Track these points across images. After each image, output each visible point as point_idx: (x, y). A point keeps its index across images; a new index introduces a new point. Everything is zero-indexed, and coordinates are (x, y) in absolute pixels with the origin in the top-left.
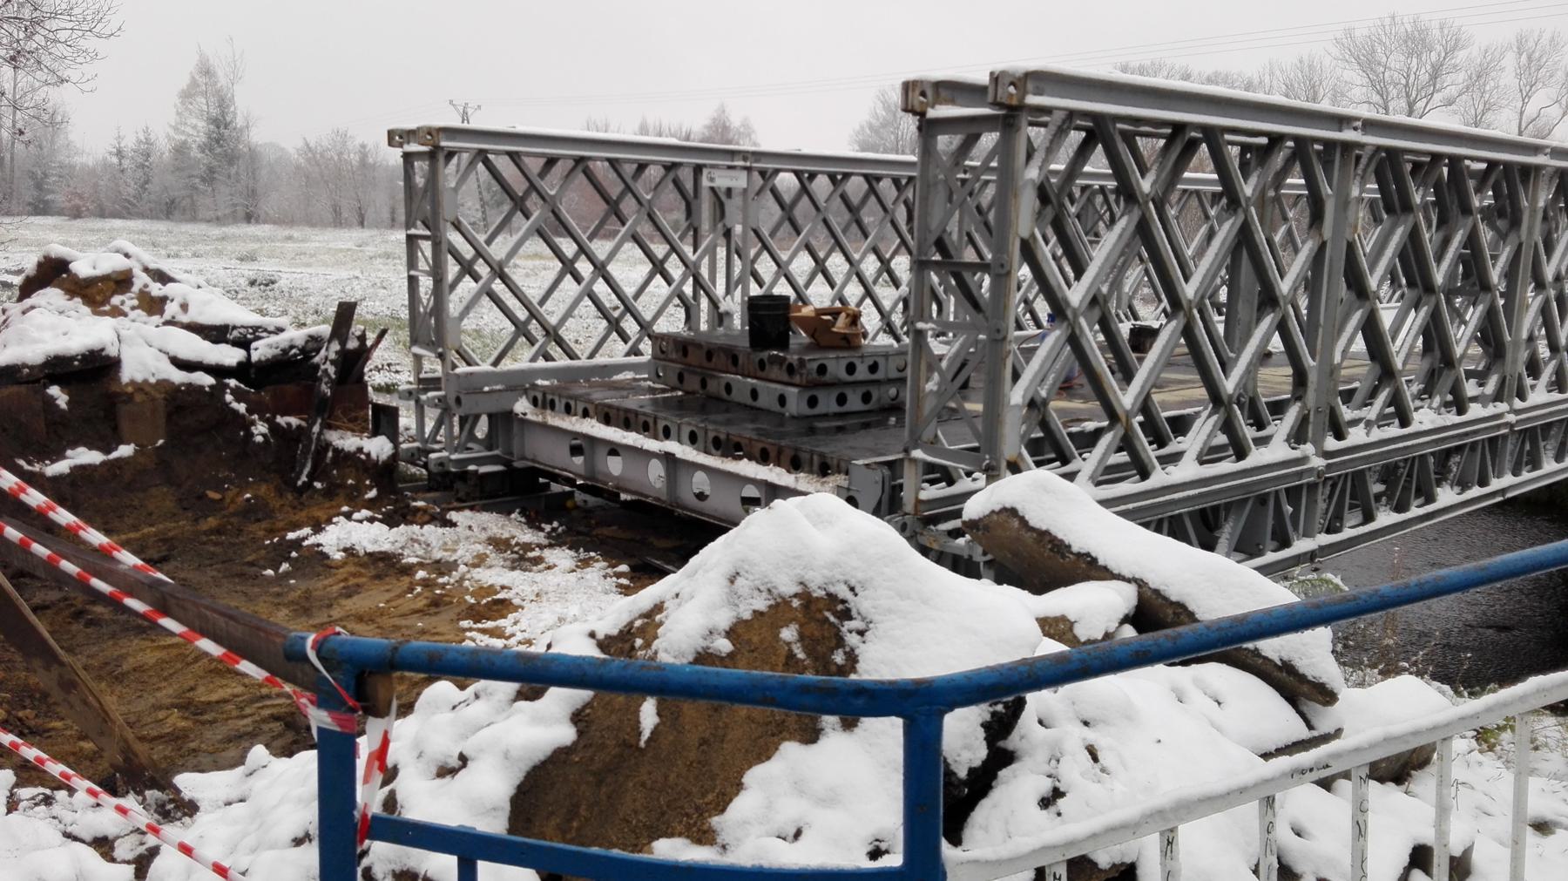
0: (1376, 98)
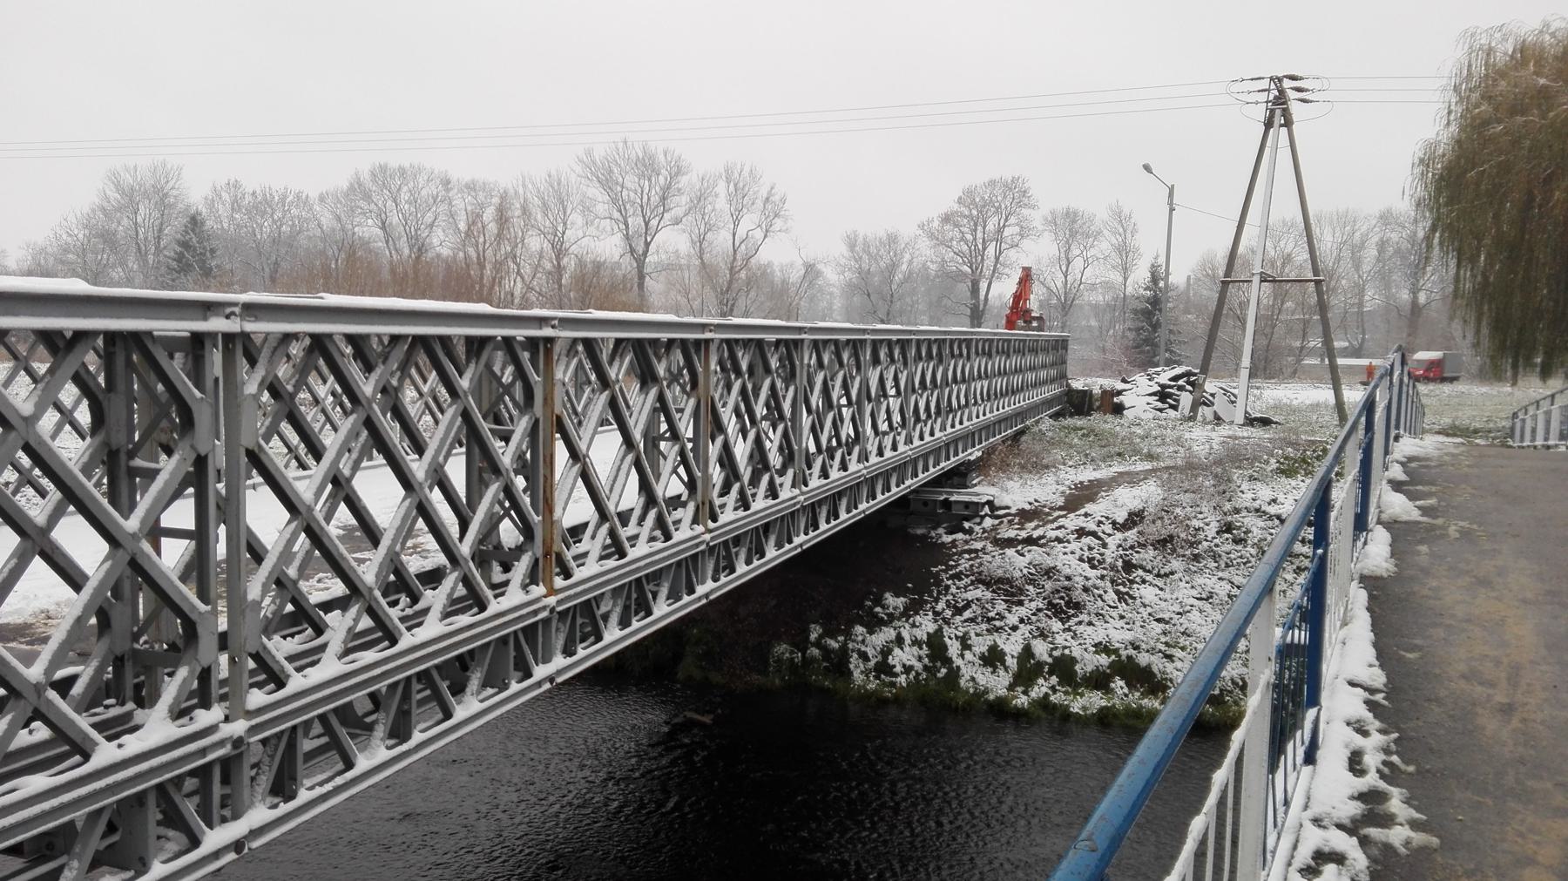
0: (616, 215)
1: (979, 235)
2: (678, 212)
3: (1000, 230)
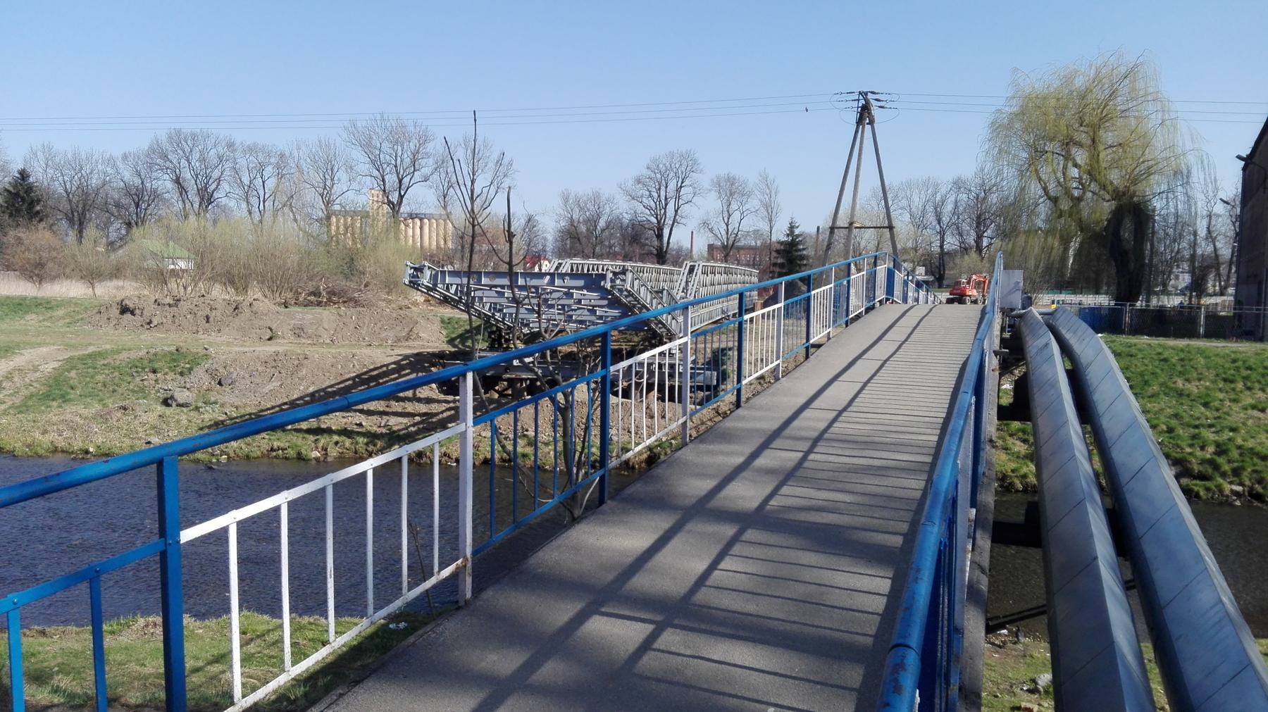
0: (376, 173)
1: (663, 193)
2: (426, 171)
3: (678, 190)
